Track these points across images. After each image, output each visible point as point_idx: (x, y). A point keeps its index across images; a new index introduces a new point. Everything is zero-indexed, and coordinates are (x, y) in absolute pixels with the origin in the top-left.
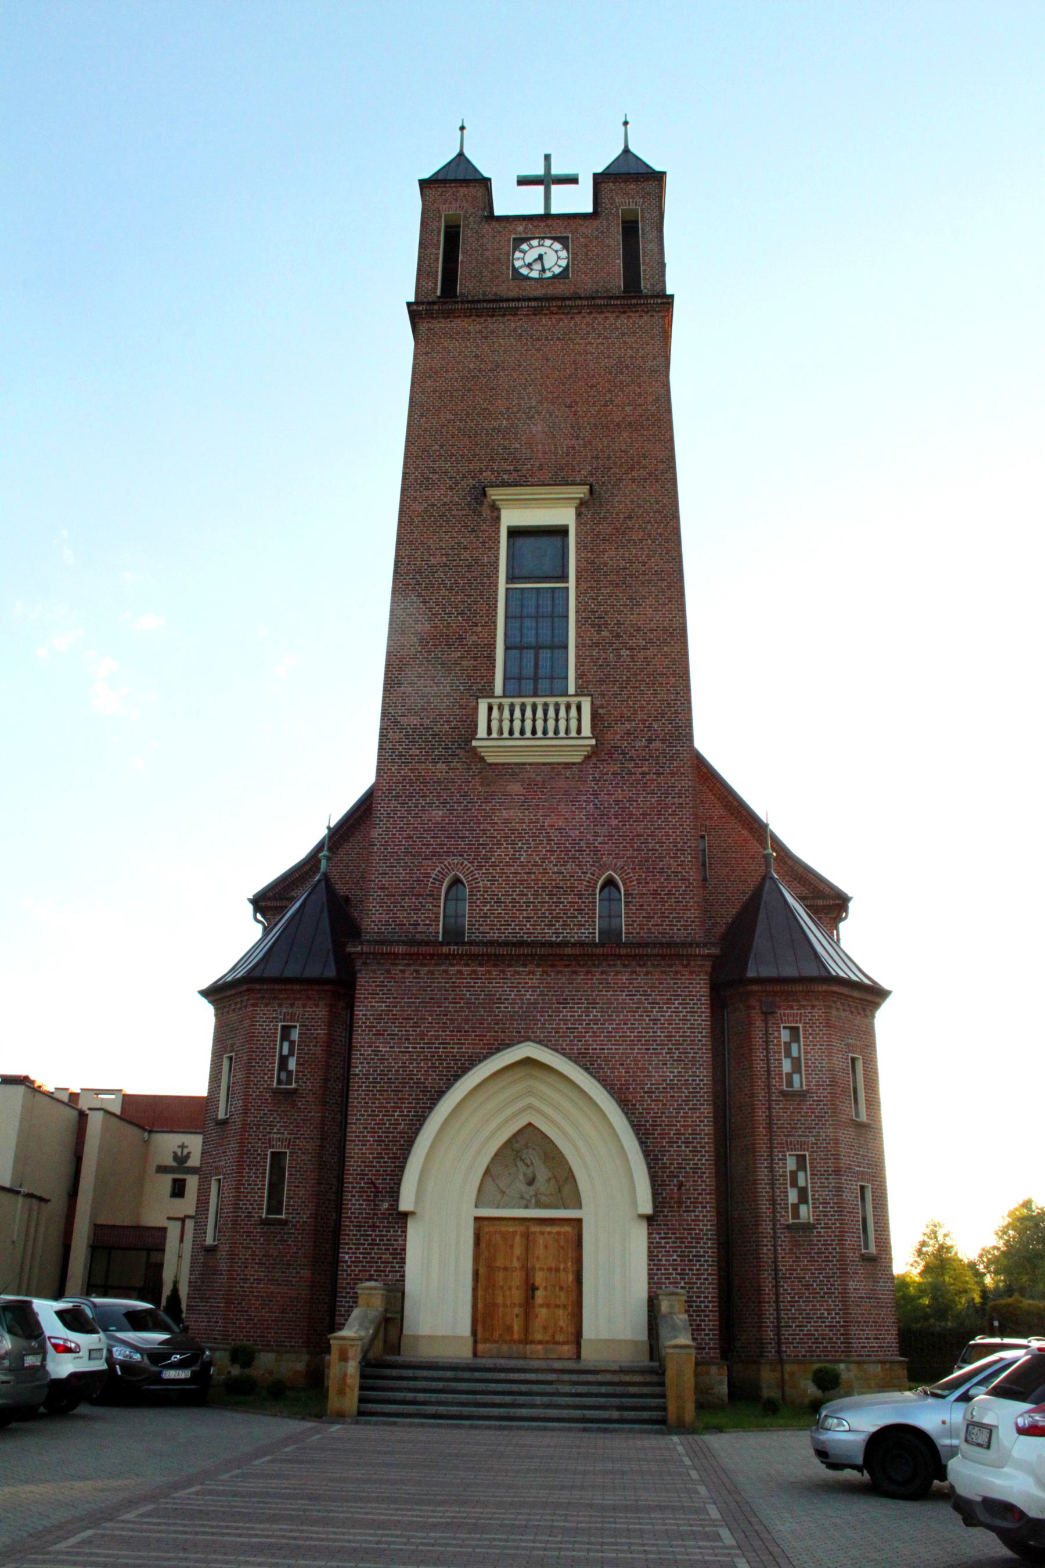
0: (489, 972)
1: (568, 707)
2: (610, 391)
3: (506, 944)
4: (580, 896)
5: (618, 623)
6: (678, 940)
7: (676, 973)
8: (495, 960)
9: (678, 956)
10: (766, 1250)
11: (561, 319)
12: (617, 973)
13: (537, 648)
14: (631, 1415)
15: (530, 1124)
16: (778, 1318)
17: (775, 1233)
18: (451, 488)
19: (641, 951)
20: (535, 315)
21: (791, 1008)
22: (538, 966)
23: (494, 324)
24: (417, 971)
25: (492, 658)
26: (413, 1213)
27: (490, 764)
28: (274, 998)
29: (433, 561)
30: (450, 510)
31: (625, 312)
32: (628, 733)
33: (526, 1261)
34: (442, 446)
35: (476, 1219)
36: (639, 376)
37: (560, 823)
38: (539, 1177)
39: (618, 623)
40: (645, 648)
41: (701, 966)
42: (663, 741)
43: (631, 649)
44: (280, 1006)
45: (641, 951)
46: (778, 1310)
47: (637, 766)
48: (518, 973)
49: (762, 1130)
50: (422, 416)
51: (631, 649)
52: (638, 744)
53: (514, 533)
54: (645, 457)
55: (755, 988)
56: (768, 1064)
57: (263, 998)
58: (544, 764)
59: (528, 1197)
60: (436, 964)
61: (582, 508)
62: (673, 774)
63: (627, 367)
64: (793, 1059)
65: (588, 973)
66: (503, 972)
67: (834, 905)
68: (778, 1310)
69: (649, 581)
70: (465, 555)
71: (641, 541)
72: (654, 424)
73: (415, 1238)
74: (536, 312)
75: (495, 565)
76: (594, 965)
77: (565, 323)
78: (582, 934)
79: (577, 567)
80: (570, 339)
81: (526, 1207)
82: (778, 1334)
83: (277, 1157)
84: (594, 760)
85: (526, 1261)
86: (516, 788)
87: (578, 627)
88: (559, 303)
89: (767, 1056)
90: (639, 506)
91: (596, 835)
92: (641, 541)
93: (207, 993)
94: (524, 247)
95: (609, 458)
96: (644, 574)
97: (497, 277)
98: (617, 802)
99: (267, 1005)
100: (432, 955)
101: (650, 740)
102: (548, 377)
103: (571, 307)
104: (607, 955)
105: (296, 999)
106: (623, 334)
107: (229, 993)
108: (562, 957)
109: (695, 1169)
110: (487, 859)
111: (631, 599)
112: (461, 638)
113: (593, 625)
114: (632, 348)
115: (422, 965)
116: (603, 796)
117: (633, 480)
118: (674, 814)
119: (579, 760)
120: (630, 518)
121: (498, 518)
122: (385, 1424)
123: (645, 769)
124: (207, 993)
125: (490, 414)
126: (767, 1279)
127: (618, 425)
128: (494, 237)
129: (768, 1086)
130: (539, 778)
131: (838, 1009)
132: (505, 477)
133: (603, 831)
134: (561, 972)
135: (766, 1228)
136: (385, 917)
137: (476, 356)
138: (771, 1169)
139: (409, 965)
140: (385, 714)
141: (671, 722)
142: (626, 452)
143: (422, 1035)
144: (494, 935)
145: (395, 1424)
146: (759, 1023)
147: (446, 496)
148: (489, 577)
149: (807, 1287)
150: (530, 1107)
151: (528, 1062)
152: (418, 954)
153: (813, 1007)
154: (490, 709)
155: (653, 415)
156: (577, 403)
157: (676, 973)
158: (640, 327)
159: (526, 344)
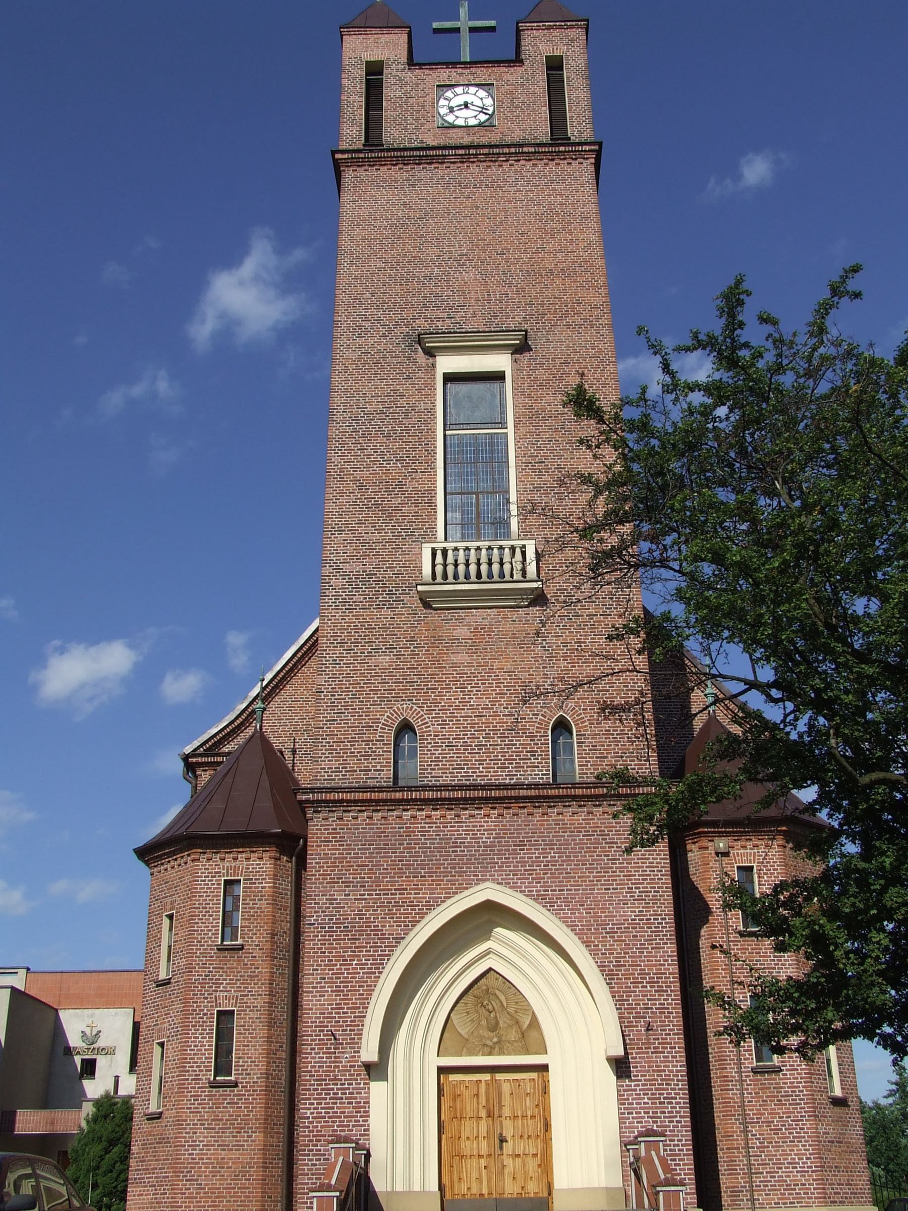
2: (541, 238)
4: (532, 738)
18: (384, 336)
20: (462, 162)
21: (744, 847)
23: (422, 173)
24: (371, 818)
25: (432, 504)
27: (436, 609)
29: (370, 408)
30: (384, 357)
31: (553, 160)
34: (373, 294)
35: (442, 1070)
36: (570, 223)
37: (508, 666)
38: (501, 1024)
53: (449, 378)
54: (579, 304)
59: (491, 1044)
63: (558, 214)
66: (459, 816)
70: (402, 402)
74: (465, 159)
77: (495, 171)
81: (490, 1054)
83: (225, 1016)
94: (449, 94)
95: (542, 304)
97: (422, 125)
98: (565, 644)
106: (552, 181)
108: (518, 799)
109: (662, 1009)
112: (401, 484)
113: (534, 470)
114: (561, 195)
116: (552, 639)
117: (568, 326)
120: (566, 363)
121: (434, 365)
125: (421, 260)
128: (417, 85)
132: (439, 324)
137: (405, 204)
143: (377, 881)
144: (447, 780)
147: (379, 344)
148: (426, 423)
149: (776, 1131)
150: (488, 952)
151: (489, 907)
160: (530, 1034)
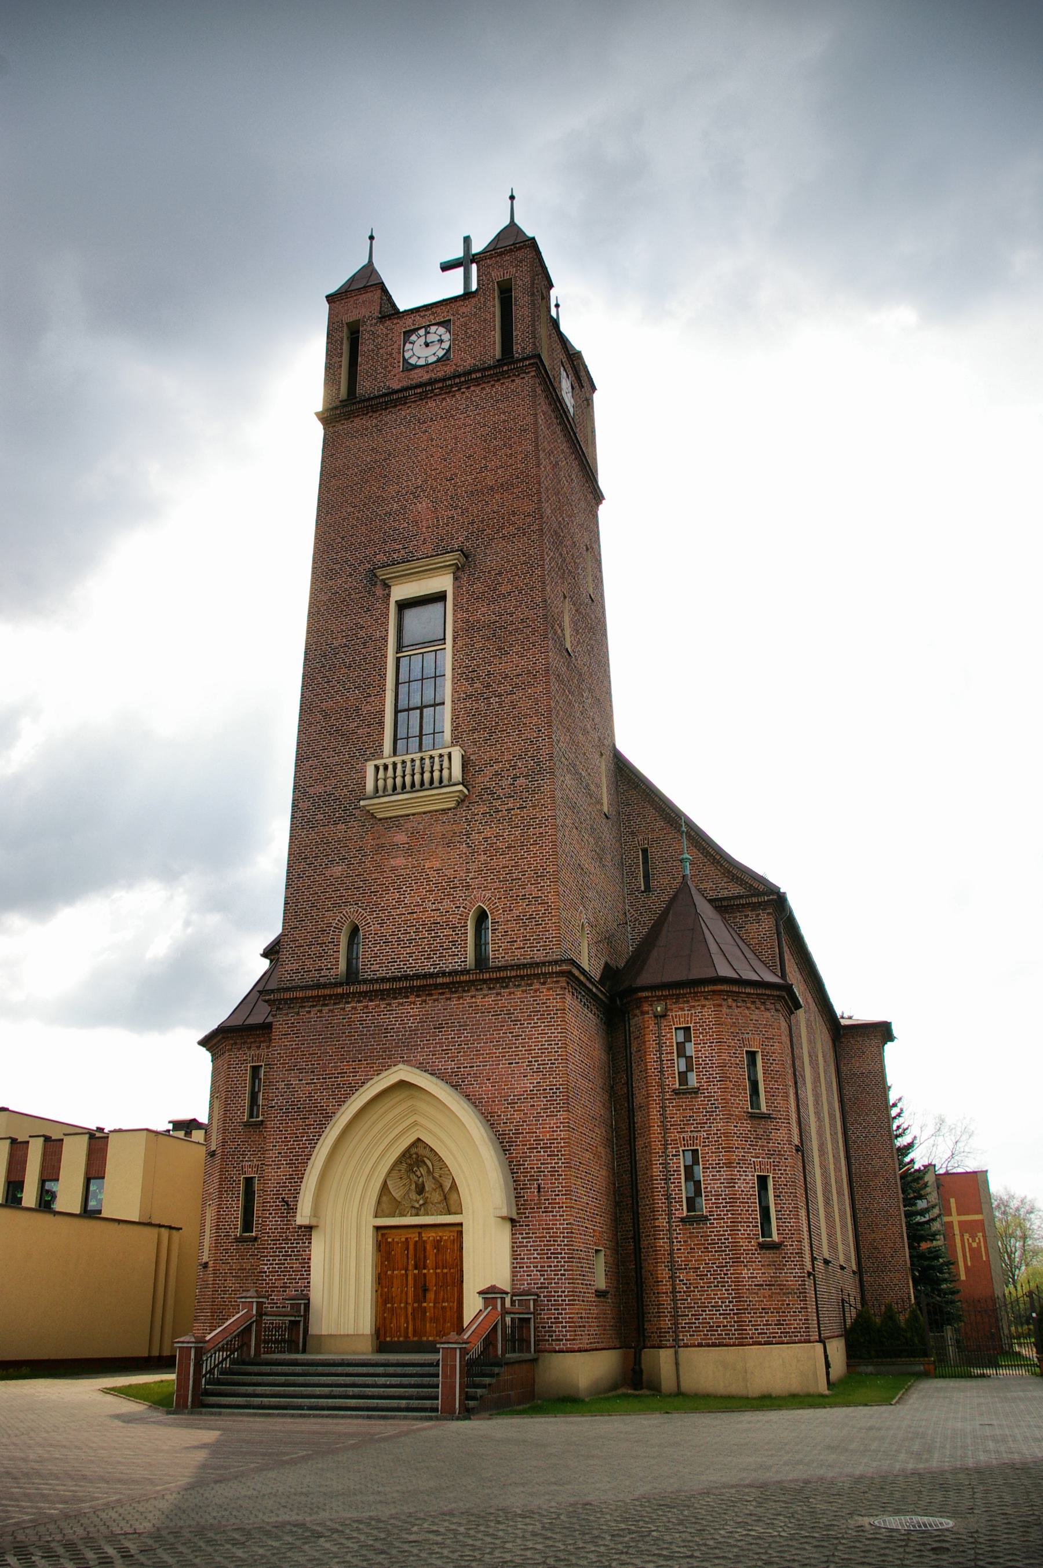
0: (378, 1006)
1: (386, 767)
2: (485, 458)
3: (394, 979)
4: (454, 929)
5: (489, 674)
6: (538, 960)
7: (536, 991)
8: (382, 995)
9: (537, 976)
10: (662, 1243)
11: (444, 399)
12: (485, 996)
13: (421, 708)
14: (415, 1403)
15: (419, 1139)
16: (675, 1308)
17: (670, 1226)
18: (351, 575)
19: (502, 974)
20: (421, 400)
21: (683, 1009)
22: (418, 996)
23: (388, 417)
24: (320, 1011)
25: (381, 723)
26: (317, 1226)
27: (380, 819)
28: (244, 1043)
29: (336, 643)
30: (350, 594)
31: (499, 380)
32: (497, 774)
33: (416, 1265)
34: (343, 538)
35: (378, 1228)
36: (510, 438)
37: (437, 865)
38: (427, 1189)
39: (489, 674)
40: (512, 693)
41: (557, 982)
42: (526, 777)
43: (500, 696)
44: (249, 1048)
45: (502, 974)
46: (674, 1300)
47: (503, 803)
48: (402, 1004)
49: (656, 1129)
50: (328, 513)
51: (500, 696)
52: (504, 783)
53: (404, 605)
54: (514, 513)
55: (644, 994)
56: (661, 1064)
57: (236, 1044)
58: (424, 813)
59: (417, 1206)
60: (335, 1004)
61: (458, 571)
62: (534, 806)
63: (500, 431)
64: (687, 1057)
65: (459, 998)
66: (389, 1004)
67: (769, 901)
68: (674, 1300)
69: (517, 630)
70: (362, 633)
71: (509, 594)
72: (522, 482)
73: (318, 1250)
74: (423, 397)
75: (385, 639)
76: (464, 991)
77: (450, 401)
78: (451, 964)
79: (454, 627)
80: (452, 416)
81: (417, 1215)
82: (676, 1324)
83: (249, 1181)
84: (467, 803)
85: (416, 1265)
86: (401, 838)
87: (454, 683)
88: (440, 385)
89: (660, 1057)
90: (509, 561)
91: (468, 871)
92: (509, 594)
93: (203, 1043)
94: (413, 338)
95: (482, 522)
96: (512, 623)
97: (390, 372)
98: (486, 839)
99: (239, 1049)
100: (330, 996)
101: (515, 778)
102: (432, 456)
103: (451, 386)
104: (473, 981)
105: (261, 1042)
106: (497, 401)
107: (214, 1042)
108: (436, 986)
109: (553, 1171)
110: (377, 904)
111: (500, 649)
112: (357, 710)
113: (467, 680)
114: (504, 413)
115: (324, 1005)
116: (475, 836)
117: (503, 537)
118: (535, 843)
119: (452, 805)
120: (500, 573)
121: (389, 595)
122: (212, 1414)
123: (511, 805)
124: (203, 1043)
125: (384, 499)
126: (663, 1273)
127: (492, 488)
128: (387, 336)
129: (661, 1085)
130: (421, 826)
131: (730, 1007)
132: (395, 556)
133: (473, 867)
134: (437, 1000)
135: (662, 1222)
136: (295, 966)
137: (373, 449)
138: (665, 1165)
139: (314, 1006)
140: (296, 788)
141: (533, 758)
142: (497, 512)
143: (324, 1067)
144: (382, 973)
145: (220, 1414)
146: (652, 1026)
147: (346, 583)
148: (380, 649)
149: (702, 1276)
150: (415, 1124)
151: (402, 1084)
152: (318, 996)
153: (703, 1006)
154: (377, 768)
155: (522, 473)
156: (456, 475)
157: (536, 991)
158: (512, 391)
159: (414, 429)
160: (449, 1197)
